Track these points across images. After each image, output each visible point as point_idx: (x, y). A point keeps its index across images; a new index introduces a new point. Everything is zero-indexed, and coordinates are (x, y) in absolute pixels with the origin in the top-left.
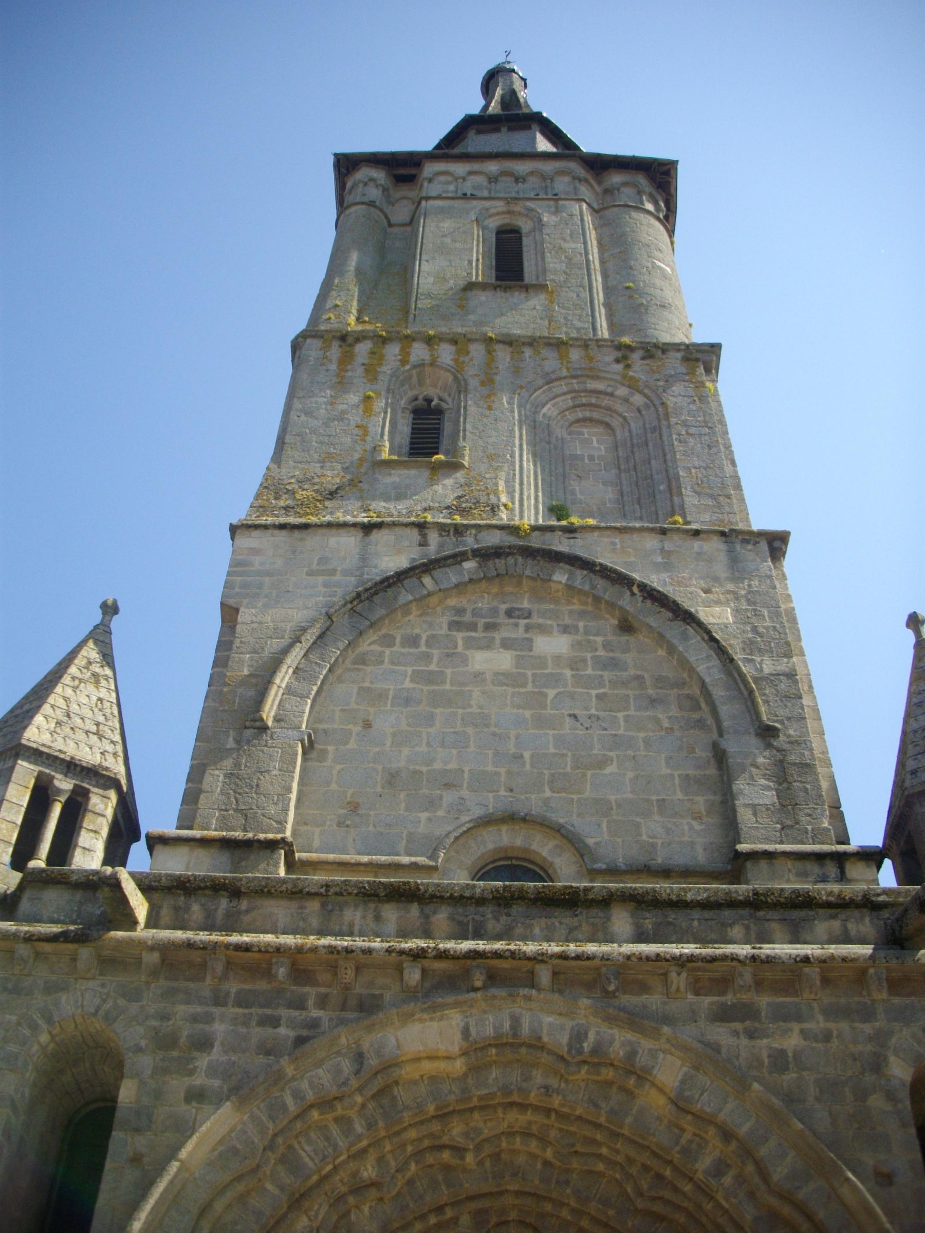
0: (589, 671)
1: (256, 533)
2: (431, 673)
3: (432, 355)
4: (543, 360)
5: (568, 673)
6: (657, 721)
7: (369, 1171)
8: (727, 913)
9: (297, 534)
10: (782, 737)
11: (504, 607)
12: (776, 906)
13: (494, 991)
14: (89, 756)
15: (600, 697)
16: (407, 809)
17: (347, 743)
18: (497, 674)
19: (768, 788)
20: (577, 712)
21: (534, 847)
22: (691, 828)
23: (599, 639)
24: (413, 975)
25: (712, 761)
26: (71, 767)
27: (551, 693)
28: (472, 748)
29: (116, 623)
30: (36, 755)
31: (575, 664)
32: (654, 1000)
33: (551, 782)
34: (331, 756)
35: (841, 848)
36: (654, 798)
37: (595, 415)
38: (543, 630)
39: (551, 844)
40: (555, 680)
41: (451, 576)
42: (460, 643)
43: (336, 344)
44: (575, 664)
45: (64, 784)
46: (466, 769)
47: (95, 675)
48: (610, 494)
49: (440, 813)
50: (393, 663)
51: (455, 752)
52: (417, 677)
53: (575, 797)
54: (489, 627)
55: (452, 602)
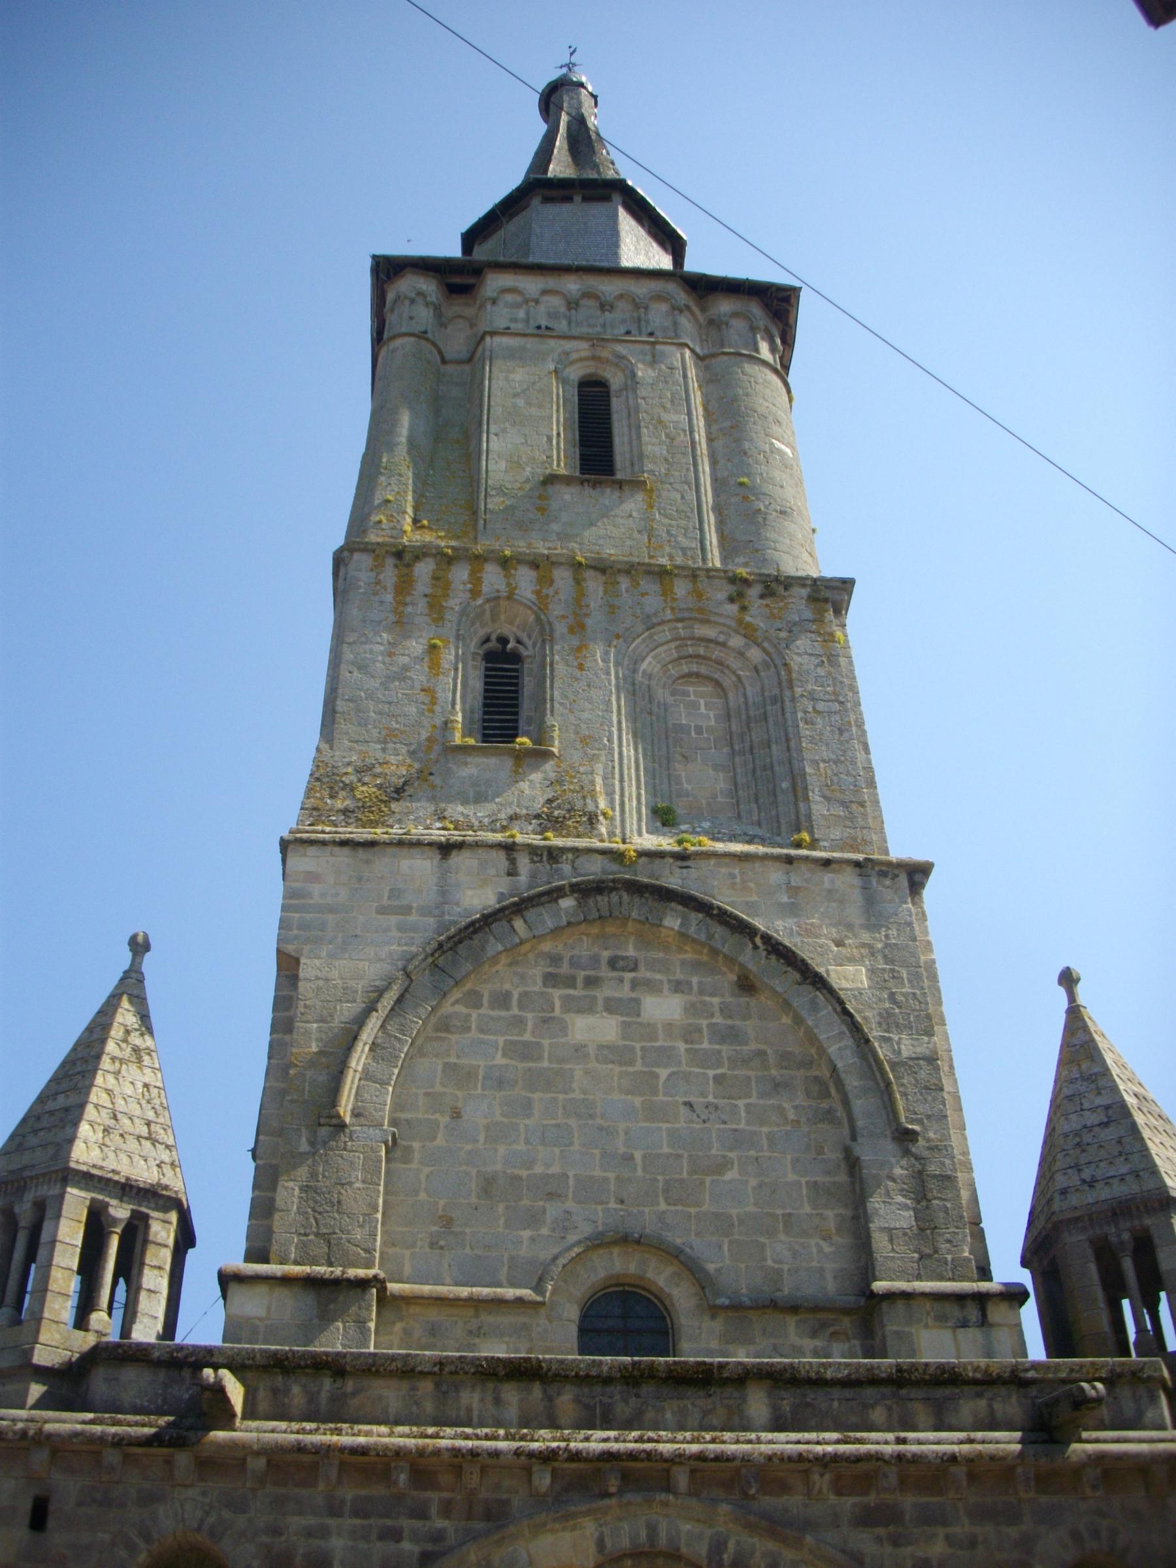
0: (705, 1045)
1: (312, 851)
2: (526, 1044)
3: (508, 584)
4: (643, 595)
5: (682, 1046)
6: (781, 1110)
8: (870, 1392)
9: (361, 853)
10: (921, 1142)
11: (606, 954)
13: (629, 1497)
14: (145, 1173)
15: (718, 1079)
16: (507, 1225)
17: (434, 1138)
18: (601, 1047)
19: (905, 1207)
20: (692, 1099)
21: (649, 1275)
22: (820, 1250)
23: (716, 1000)
24: (543, 1480)
25: (843, 1165)
26: (127, 1189)
27: (663, 1073)
28: (576, 1147)
29: (149, 964)
30: (87, 1179)
31: (690, 1034)
32: (794, 1502)
33: (666, 1191)
34: (417, 1155)
35: (984, 1286)
36: (779, 1212)
37: (703, 670)
38: (652, 987)
39: (669, 1270)
40: (665, 1056)
41: (546, 918)
42: (558, 1003)
43: (390, 561)
44: (690, 1034)
45: (120, 1211)
46: (571, 1174)
47: (136, 1050)
48: (721, 783)
49: (545, 1231)
50: (482, 1031)
51: (557, 1150)
52: (511, 1049)
53: (693, 1210)
54: (591, 982)
55: (547, 946)
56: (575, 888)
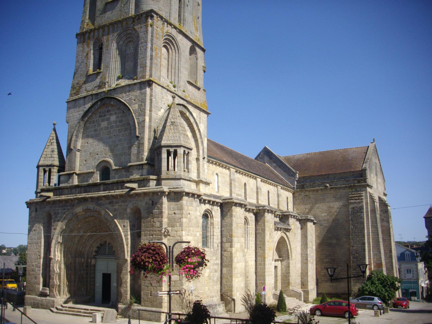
0: (118, 124)
5: (115, 125)
6: (126, 134)
7: (80, 226)
8: (114, 184)
10: (140, 137)
12: (120, 183)
14: (49, 163)
15: (119, 130)
18: (105, 127)
20: (115, 134)
23: (120, 115)
24: (76, 201)
26: (47, 166)
27: (112, 130)
29: (56, 126)
30: (42, 166)
38: (111, 115)
40: (112, 127)
41: (96, 107)
44: (116, 122)
45: (47, 169)
54: (105, 116)
55: (99, 111)
56: (100, 100)
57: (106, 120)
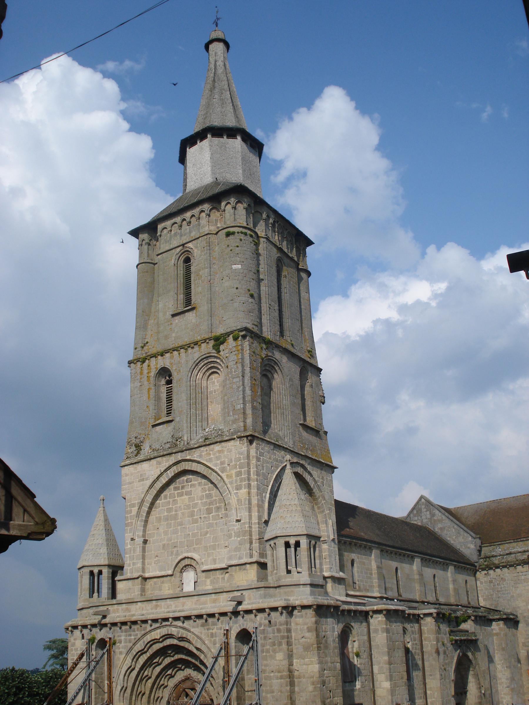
5: (200, 501)
23: (207, 487)
27: (196, 510)
50: (162, 507)
54: (183, 487)
57: (186, 494)
